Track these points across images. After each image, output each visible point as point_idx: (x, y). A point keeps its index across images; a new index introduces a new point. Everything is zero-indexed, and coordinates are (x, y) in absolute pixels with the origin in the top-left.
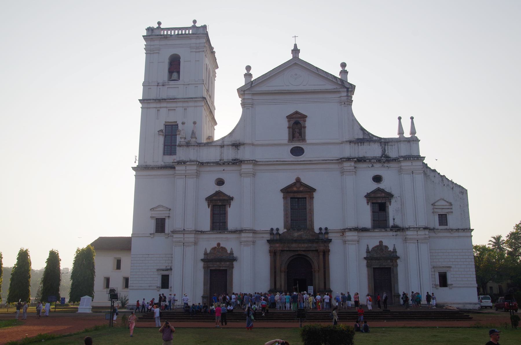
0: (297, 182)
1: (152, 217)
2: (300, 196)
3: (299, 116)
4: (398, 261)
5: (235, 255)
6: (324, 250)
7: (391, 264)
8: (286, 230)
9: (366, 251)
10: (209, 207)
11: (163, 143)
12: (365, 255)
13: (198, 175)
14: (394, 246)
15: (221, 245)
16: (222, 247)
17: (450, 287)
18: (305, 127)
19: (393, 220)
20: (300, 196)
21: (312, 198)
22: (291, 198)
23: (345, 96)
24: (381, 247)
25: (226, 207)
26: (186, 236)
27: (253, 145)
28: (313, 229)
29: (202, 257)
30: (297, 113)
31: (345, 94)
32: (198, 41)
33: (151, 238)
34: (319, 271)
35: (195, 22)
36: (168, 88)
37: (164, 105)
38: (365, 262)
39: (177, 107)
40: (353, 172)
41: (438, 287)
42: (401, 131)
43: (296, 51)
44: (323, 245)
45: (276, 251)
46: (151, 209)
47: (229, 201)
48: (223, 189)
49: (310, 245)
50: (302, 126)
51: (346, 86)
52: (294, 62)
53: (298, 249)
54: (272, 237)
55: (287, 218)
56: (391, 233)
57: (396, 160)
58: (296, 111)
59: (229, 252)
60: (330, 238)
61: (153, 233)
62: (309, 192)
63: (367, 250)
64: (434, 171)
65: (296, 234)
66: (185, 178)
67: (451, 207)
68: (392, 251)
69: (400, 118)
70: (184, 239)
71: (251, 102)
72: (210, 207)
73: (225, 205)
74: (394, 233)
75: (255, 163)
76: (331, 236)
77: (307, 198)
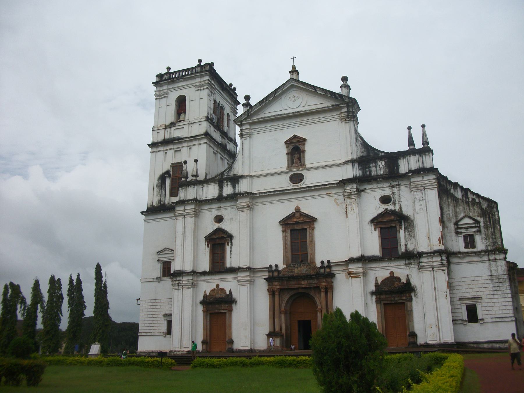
0: (296, 212)
1: (158, 261)
3: (298, 140)
4: (413, 294)
5: (234, 295)
6: (326, 286)
7: (404, 298)
8: (285, 266)
9: (374, 284)
10: (208, 247)
12: (373, 288)
13: (196, 214)
15: (220, 287)
16: (220, 288)
17: (481, 323)
18: (304, 151)
19: (404, 246)
20: (301, 228)
21: (313, 228)
22: (291, 231)
23: (346, 112)
24: (392, 279)
27: (250, 176)
28: (315, 263)
29: (201, 298)
30: (295, 137)
31: (345, 110)
32: (202, 79)
33: (159, 282)
35: (200, 61)
36: (174, 129)
37: (171, 147)
38: (374, 298)
39: (182, 147)
40: (355, 194)
41: (465, 323)
42: (411, 142)
43: (294, 71)
44: (325, 281)
45: (274, 290)
46: (157, 253)
48: (223, 225)
49: (311, 281)
50: (301, 150)
51: (346, 101)
54: (271, 274)
55: (286, 252)
56: (402, 262)
57: (405, 176)
58: (295, 135)
60: (332, 272)
61: (159, 276)
62: (309, 221)
63: (375, 284)
64: (456, 185)
65: (296, 271)
67: (478, 225)
68: (405, 282)
69: (409, 128)
71: (248, 131)
72: (209, 247)
73: (224, 243)
74: (407, 262)
75: (250, 195)
76: (334, 269)
77: (308, 230)
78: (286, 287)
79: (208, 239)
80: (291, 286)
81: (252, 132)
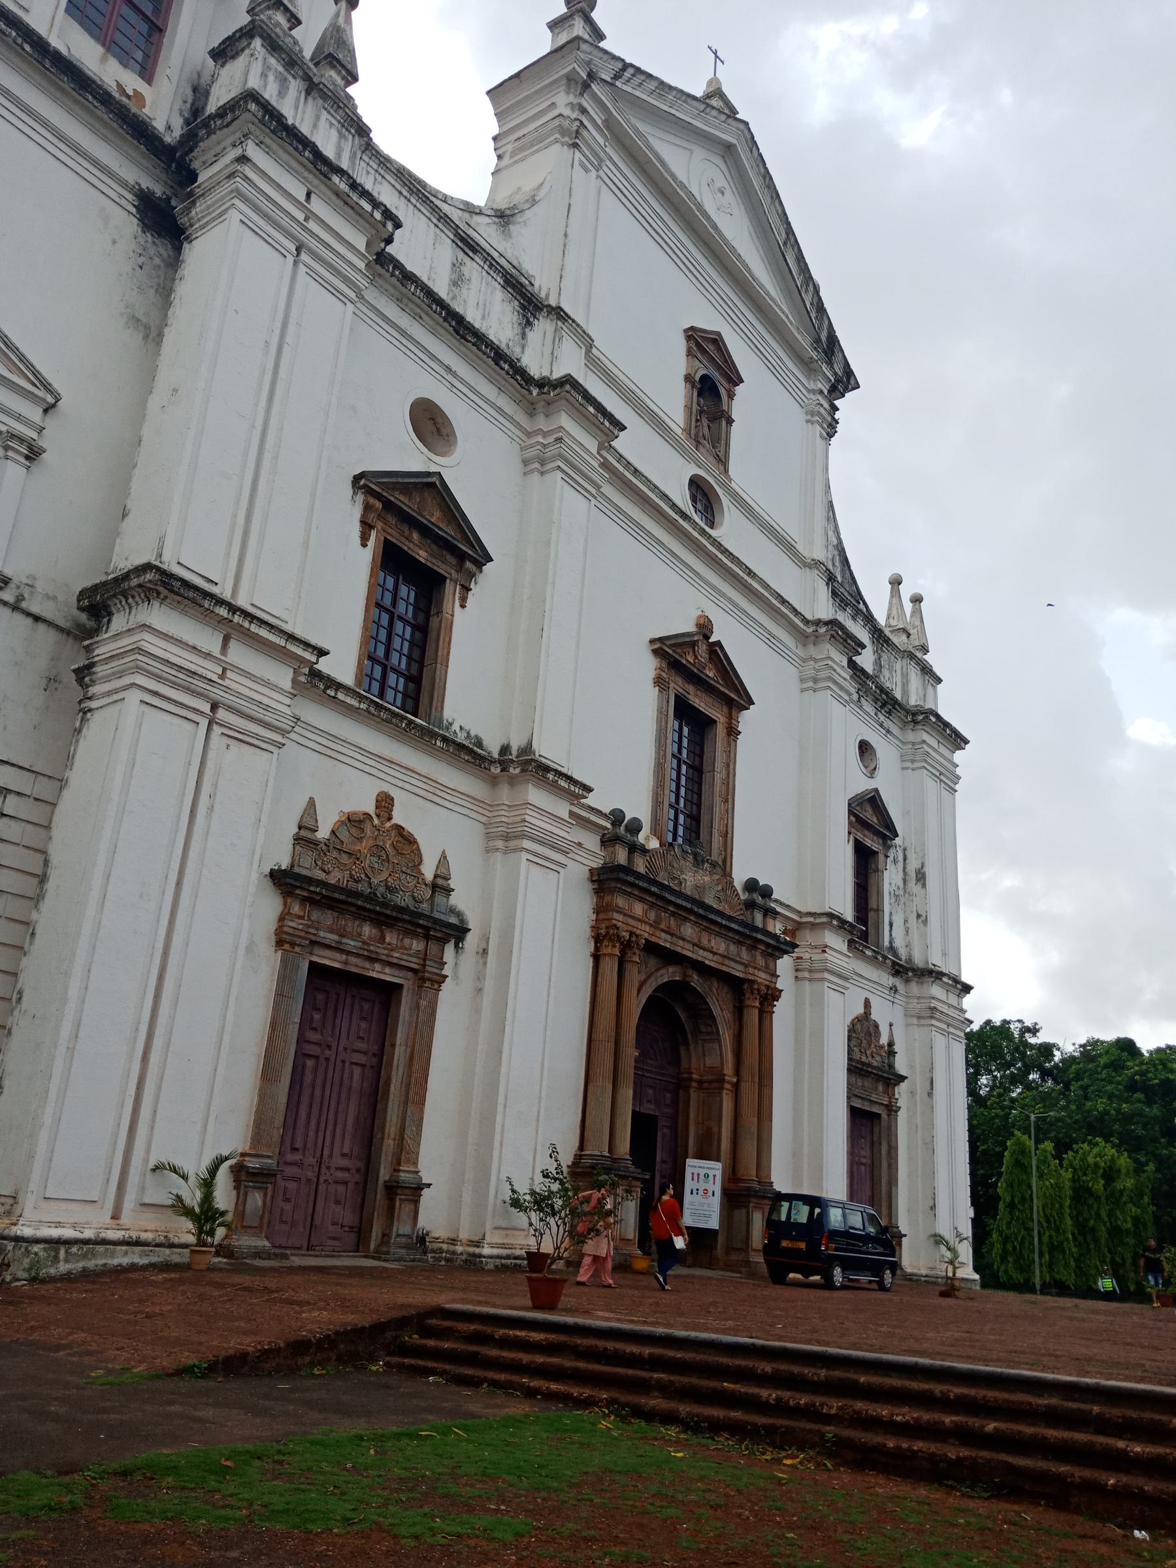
14: (891, 1029)
16: (399, 829)
18: (730, 421)
21: (733, 732)
26: (239, 654)
30: (717, 341)
34: (737, 1086)
52: (734, 141)
53: (700, 955)
58: (719, 334)
59: (428, 871)
70: (222, 676)
77: (721, 731)
78: (664, 941)
79: (378, 496)
80: (681, 943)
81: (605, 168)
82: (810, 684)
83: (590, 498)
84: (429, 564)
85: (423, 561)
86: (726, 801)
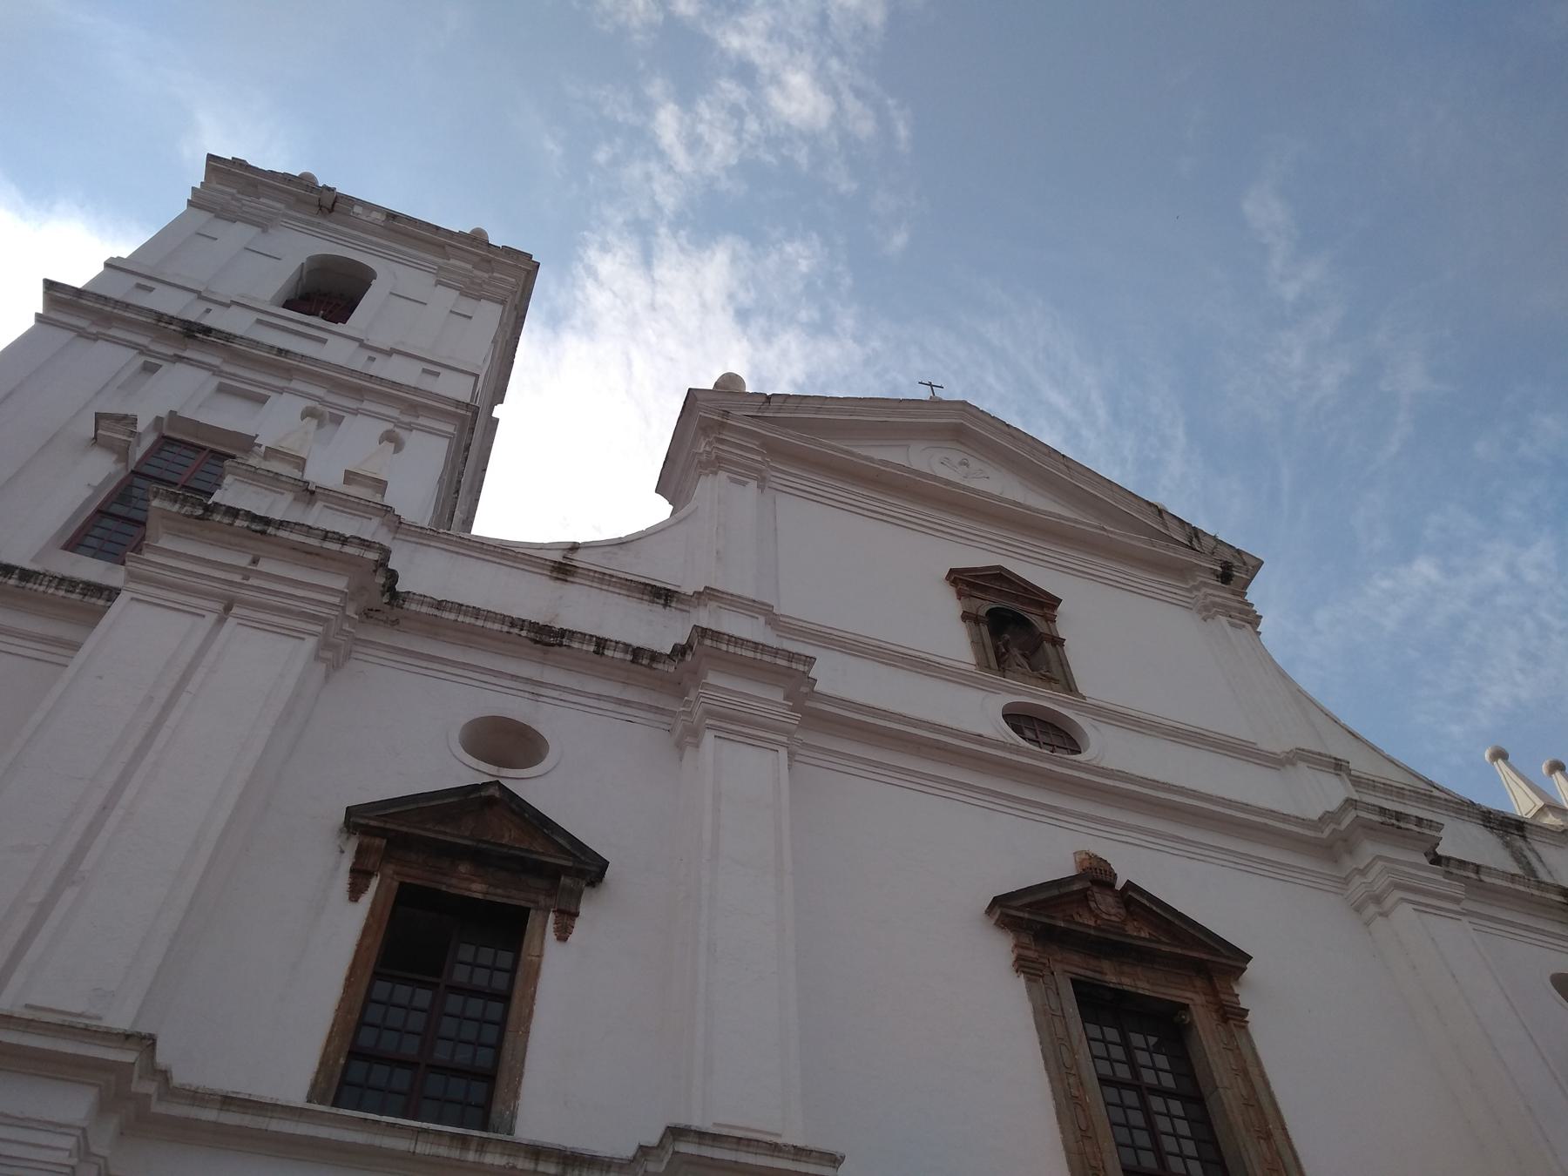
2: (1139, 984)
10: (355, 893)
11: (96, 482)
18: (1058, 642)
21: (1232, 1016)
25: (534, 919)
30: (1000, 576)
39: (281, 391)
47: (565, 881)
66: (212, 618)
72: (367, 899)
77: (1203, 1020)
81: (772, 479)
82: (1372, 909)
83: (776, 747)
84: (489, 898)
85: (480, 896)
86: (1268, 1136)
